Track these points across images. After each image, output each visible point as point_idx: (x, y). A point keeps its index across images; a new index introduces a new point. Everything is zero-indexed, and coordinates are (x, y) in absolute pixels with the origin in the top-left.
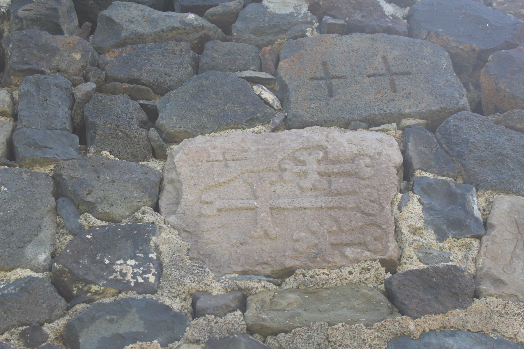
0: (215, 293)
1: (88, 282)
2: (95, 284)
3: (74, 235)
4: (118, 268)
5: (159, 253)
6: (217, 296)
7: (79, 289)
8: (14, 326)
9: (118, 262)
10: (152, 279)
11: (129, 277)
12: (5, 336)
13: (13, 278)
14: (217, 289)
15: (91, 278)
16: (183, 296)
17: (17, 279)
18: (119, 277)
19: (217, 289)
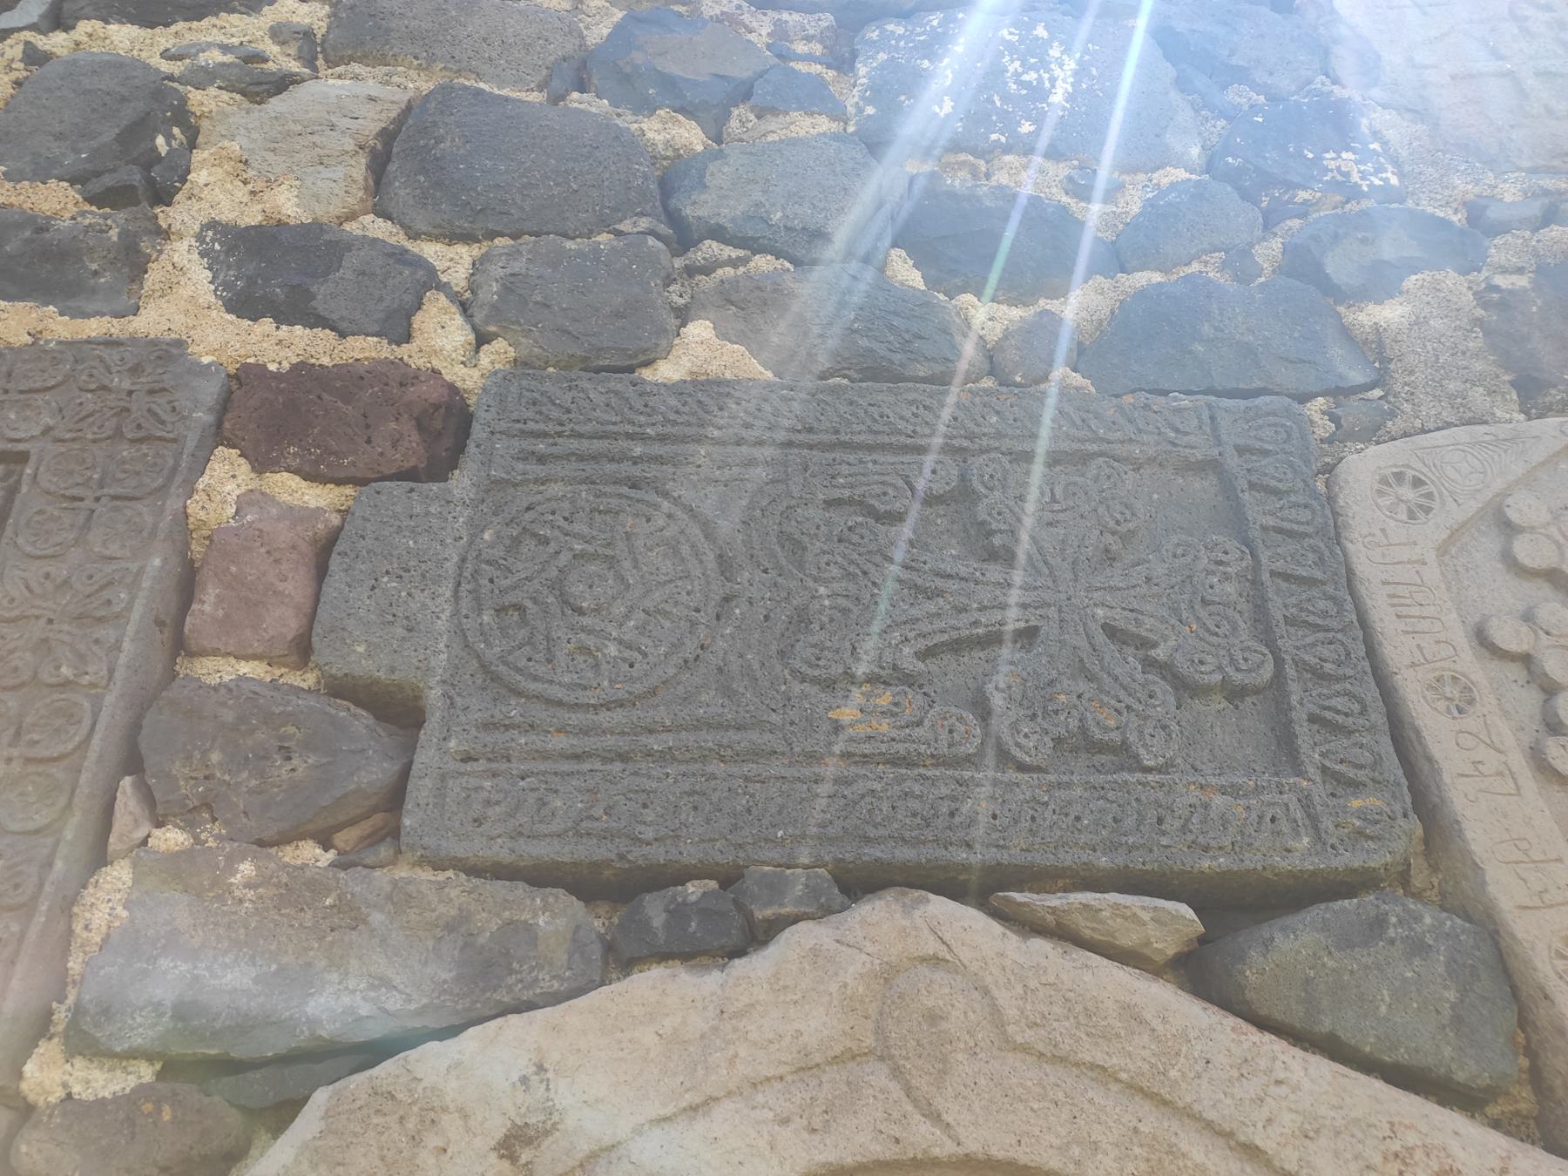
0: (1508, 198)
1: (1292, 186)
2: (1305, 188)
3: (1229, 119)
4: (1332, 165)
5: (1385, 143)
6: (1513, 203)
7: (1273, 198)
8: (1206, 252)
9: (1327, 156)
10: (1394, 181)
11: (1355, 178)
12: (1195, 267)
13: (1165, 181)
14: (1510, 192)
15: (1297, 179)
16: (1454, 205)
17: (1172, 183)
18: (1339, 178)
19: (1510, 192)
